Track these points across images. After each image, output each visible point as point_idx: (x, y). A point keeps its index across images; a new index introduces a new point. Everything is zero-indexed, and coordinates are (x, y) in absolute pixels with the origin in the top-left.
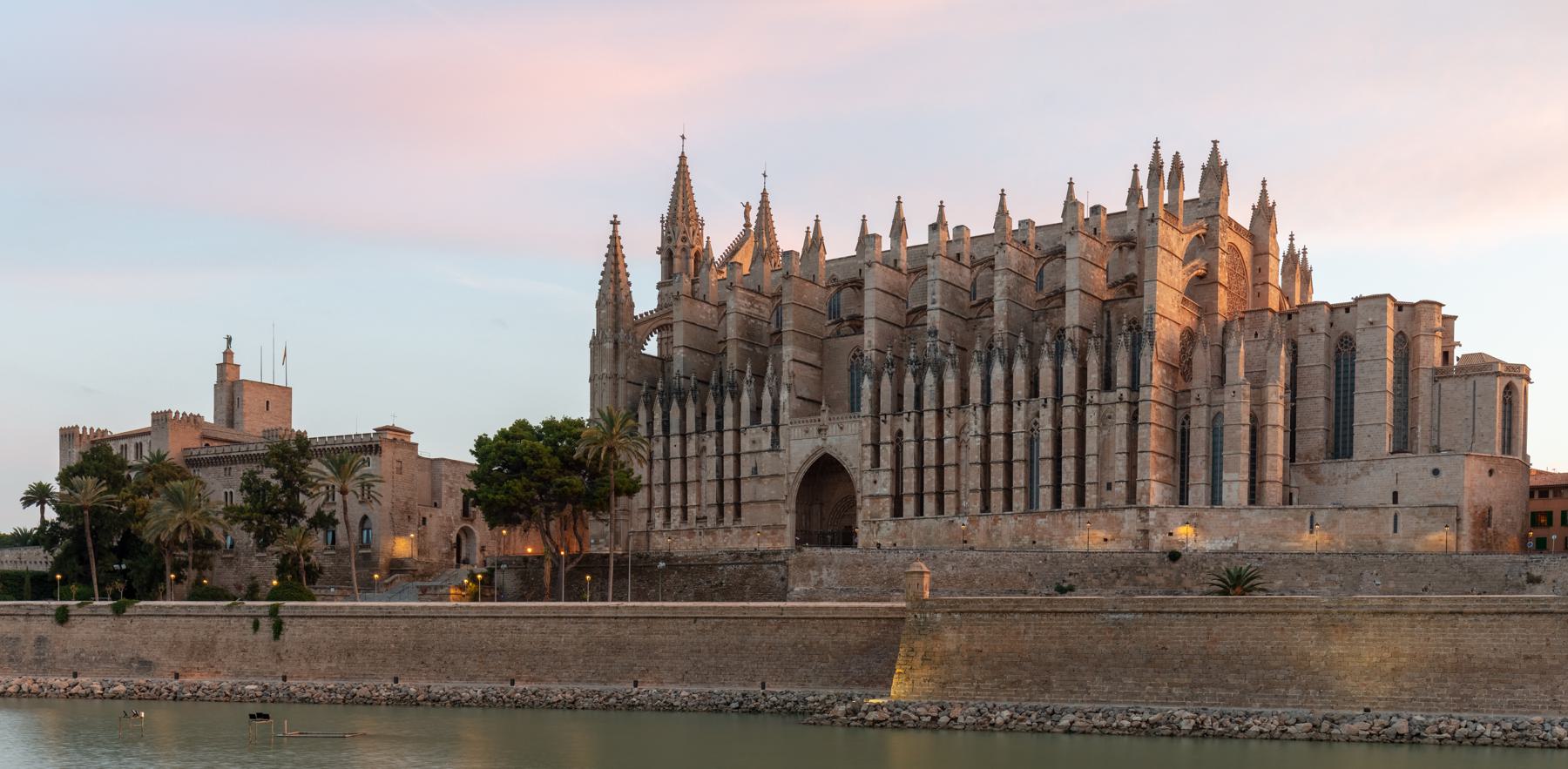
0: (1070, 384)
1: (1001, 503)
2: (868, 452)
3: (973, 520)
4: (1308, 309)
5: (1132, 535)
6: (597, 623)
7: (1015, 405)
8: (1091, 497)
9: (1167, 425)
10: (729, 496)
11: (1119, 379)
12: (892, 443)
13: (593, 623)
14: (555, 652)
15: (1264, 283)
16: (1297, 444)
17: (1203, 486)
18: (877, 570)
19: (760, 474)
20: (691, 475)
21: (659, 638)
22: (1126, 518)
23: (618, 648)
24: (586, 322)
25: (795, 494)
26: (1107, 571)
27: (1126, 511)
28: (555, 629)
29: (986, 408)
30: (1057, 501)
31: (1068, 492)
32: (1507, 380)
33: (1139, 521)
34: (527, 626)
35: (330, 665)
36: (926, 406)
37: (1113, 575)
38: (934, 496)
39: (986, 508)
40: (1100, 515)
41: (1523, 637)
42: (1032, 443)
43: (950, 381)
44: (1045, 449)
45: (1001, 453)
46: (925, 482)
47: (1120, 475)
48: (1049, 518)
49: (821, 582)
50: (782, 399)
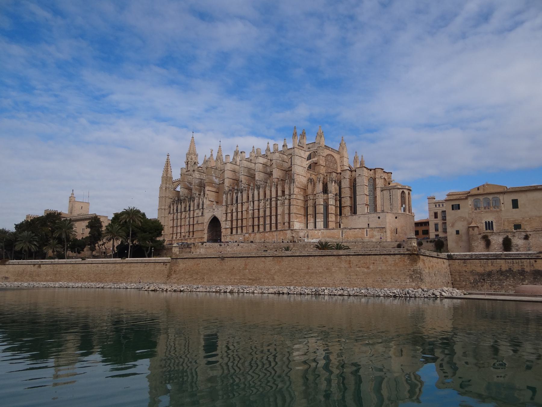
0: (274, 195)
2: (225, 215)
3: (250, 234)
4: (344, 171)
5: (290, 238)
7: (260, 201)
8: (280, 227)
10: (191, 230)
12: (231, 213)
13: (117, 264)
15: (343, 165)
19: (199, 223)
20: (183, 224)
21: (132, 268)
22: (288, 233)
23: (122, 272)
24: (158, 182)
25: (207, 228)
29: (253, 202)
32: (402, 190)
34: (100, 265)
36: (239, 202)
37: (281, 249)
38: (240, 228)
40: (281, 232)
41: (326, 262)
42: (265, 211)
44: (268, 213)
46: (238, 224)
49: (200, 253)
50: (204, 201)
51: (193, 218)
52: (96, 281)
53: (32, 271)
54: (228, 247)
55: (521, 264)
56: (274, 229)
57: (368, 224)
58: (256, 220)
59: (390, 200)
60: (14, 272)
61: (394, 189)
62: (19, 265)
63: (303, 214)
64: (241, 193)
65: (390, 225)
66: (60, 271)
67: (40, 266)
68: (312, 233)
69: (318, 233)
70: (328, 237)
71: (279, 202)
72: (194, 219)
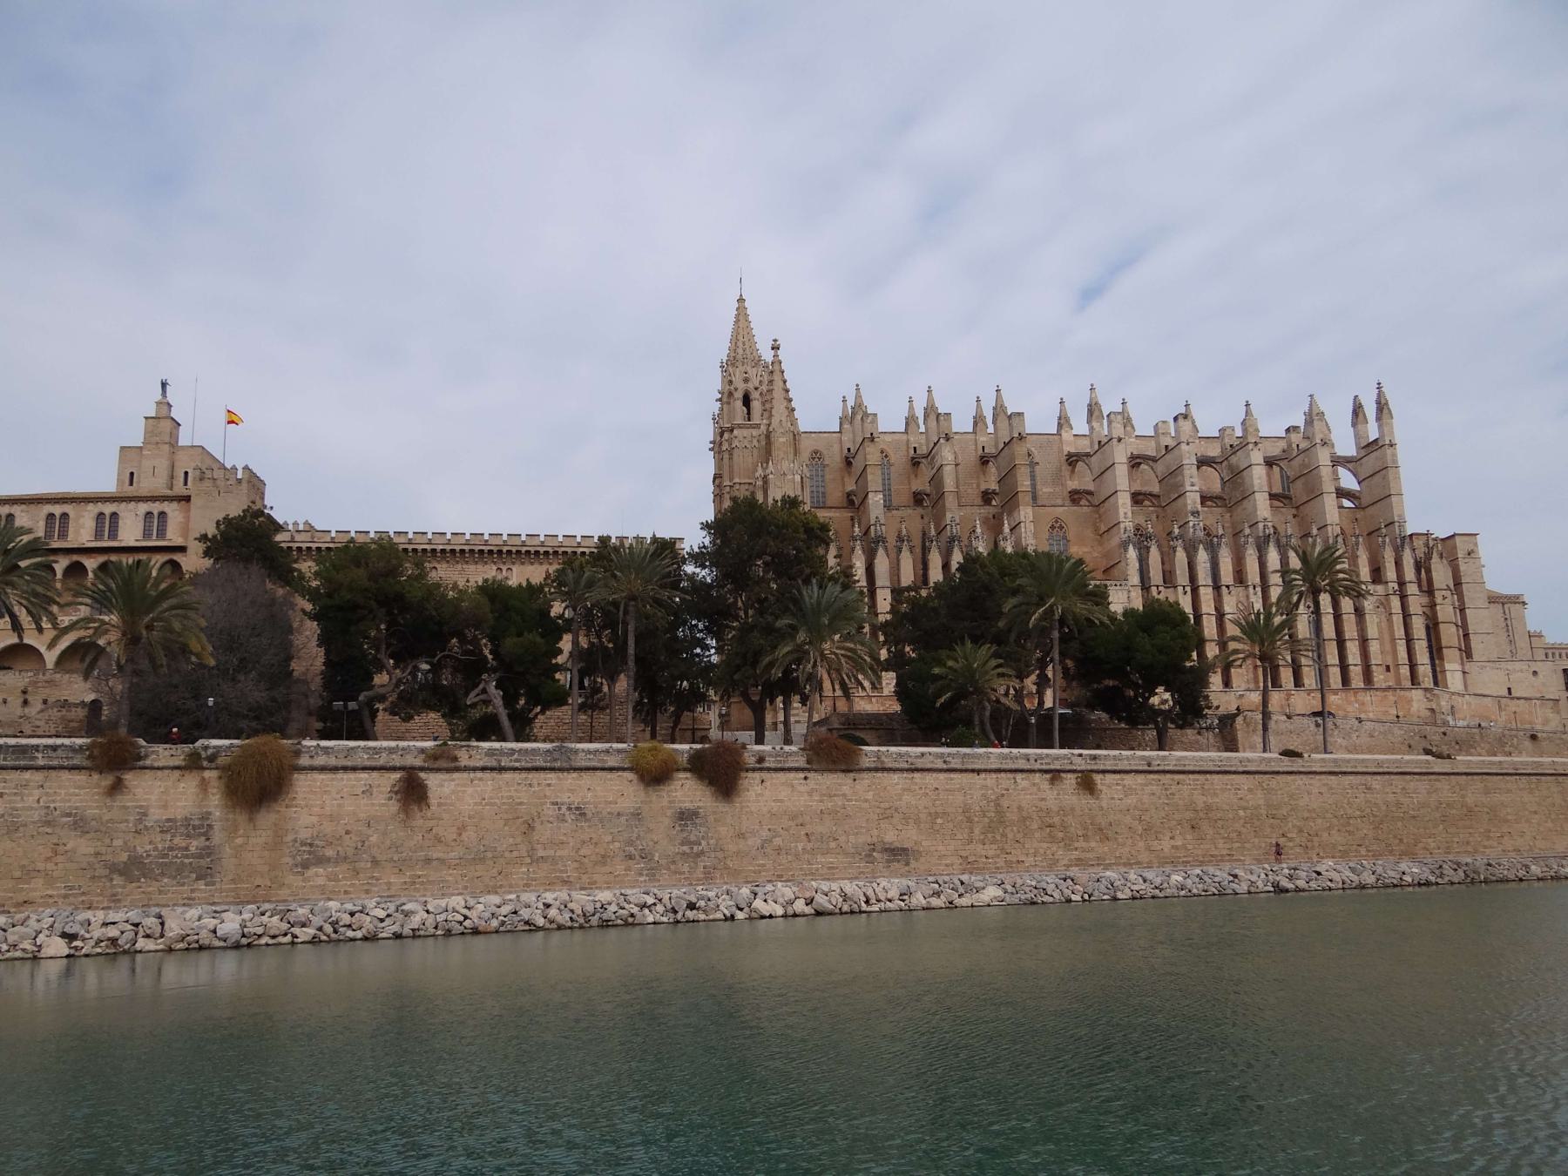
6: (1439, 780)
8: (1379, 677)
11: (1388, 574)
13: (1435, 780)
14: (1414, 817)
18: (1305, 738)
22: (1414, 698)
23: (1470, 812)
26: (1453, 743)
28: (1404, 789)
30: (1346, 680)
31: (1356, 672)
34: (1376, 782)
35: (1172, 842)
36: (1201, 582)
37: (1457, 747)
39: (1276, 683)
40: (1390, 693)
43: (1226, 560)
48: (1341, 695)
52: (1391, 852)
53: (1055, 809)
54: (1336, 732)
57: (1509, 689)
59: (1508, 631)
60: (937, 815)
61: (1515, 603)
62: (952, 775)
66: (1209, 808)
67: (1087, 783)
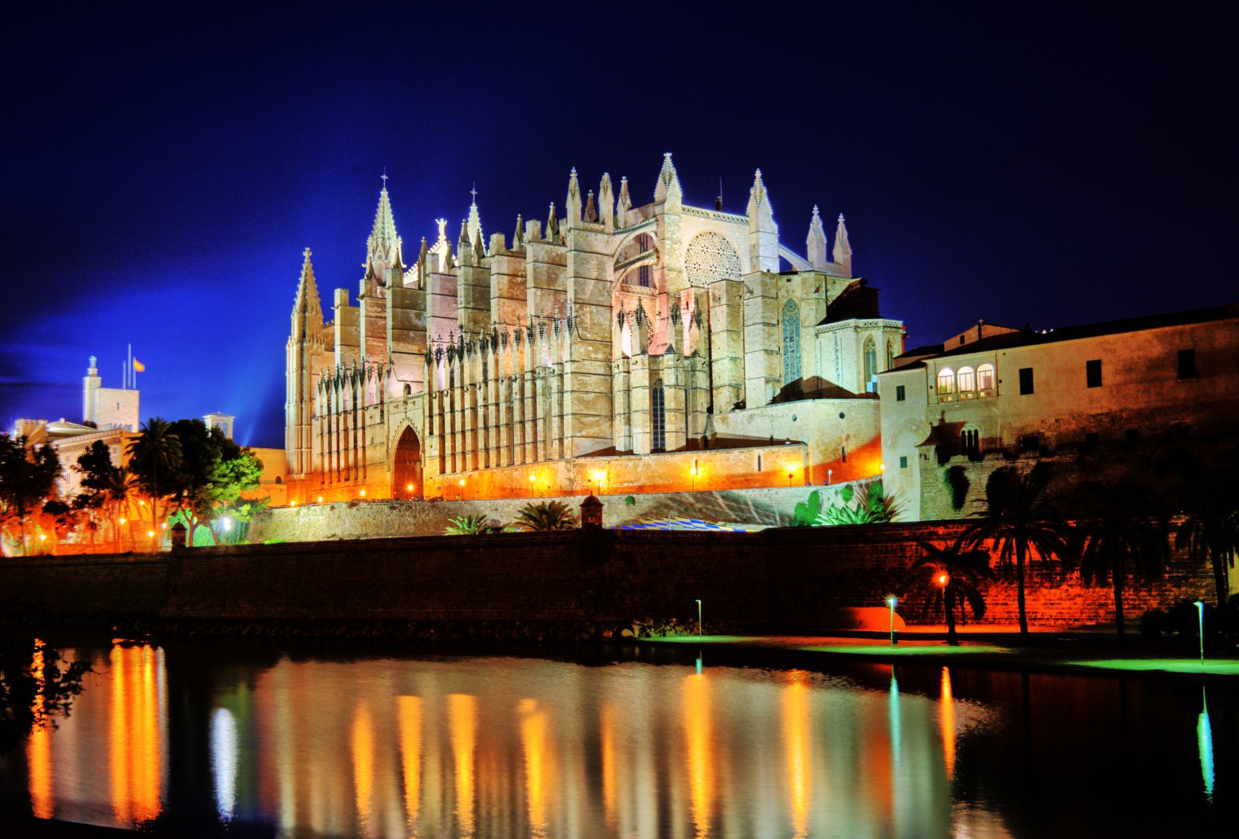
1: (495, 460)
8: (541, 453)
9: (596, 390)
16: (714, 399)
17: (623, 438)
22: (559, 470)
25: (392, 458)
27: (559, 463)
29: (487, 386)
33: (566, 471)
36: (456, 386)
42: (510, 410)
45: (494, 420)
47: (555, 434)
51: (363, 428)
55: (900, 555)
56: (529, 460)
58: (492, 432)
59: (837, 364)
63: (604, 413)
64: (461, 358)
65: (822, 438)
68: (619, 467)
69: (636, 466)
70: (661, 478)
71: (539, 383)
72: (364, 433)
